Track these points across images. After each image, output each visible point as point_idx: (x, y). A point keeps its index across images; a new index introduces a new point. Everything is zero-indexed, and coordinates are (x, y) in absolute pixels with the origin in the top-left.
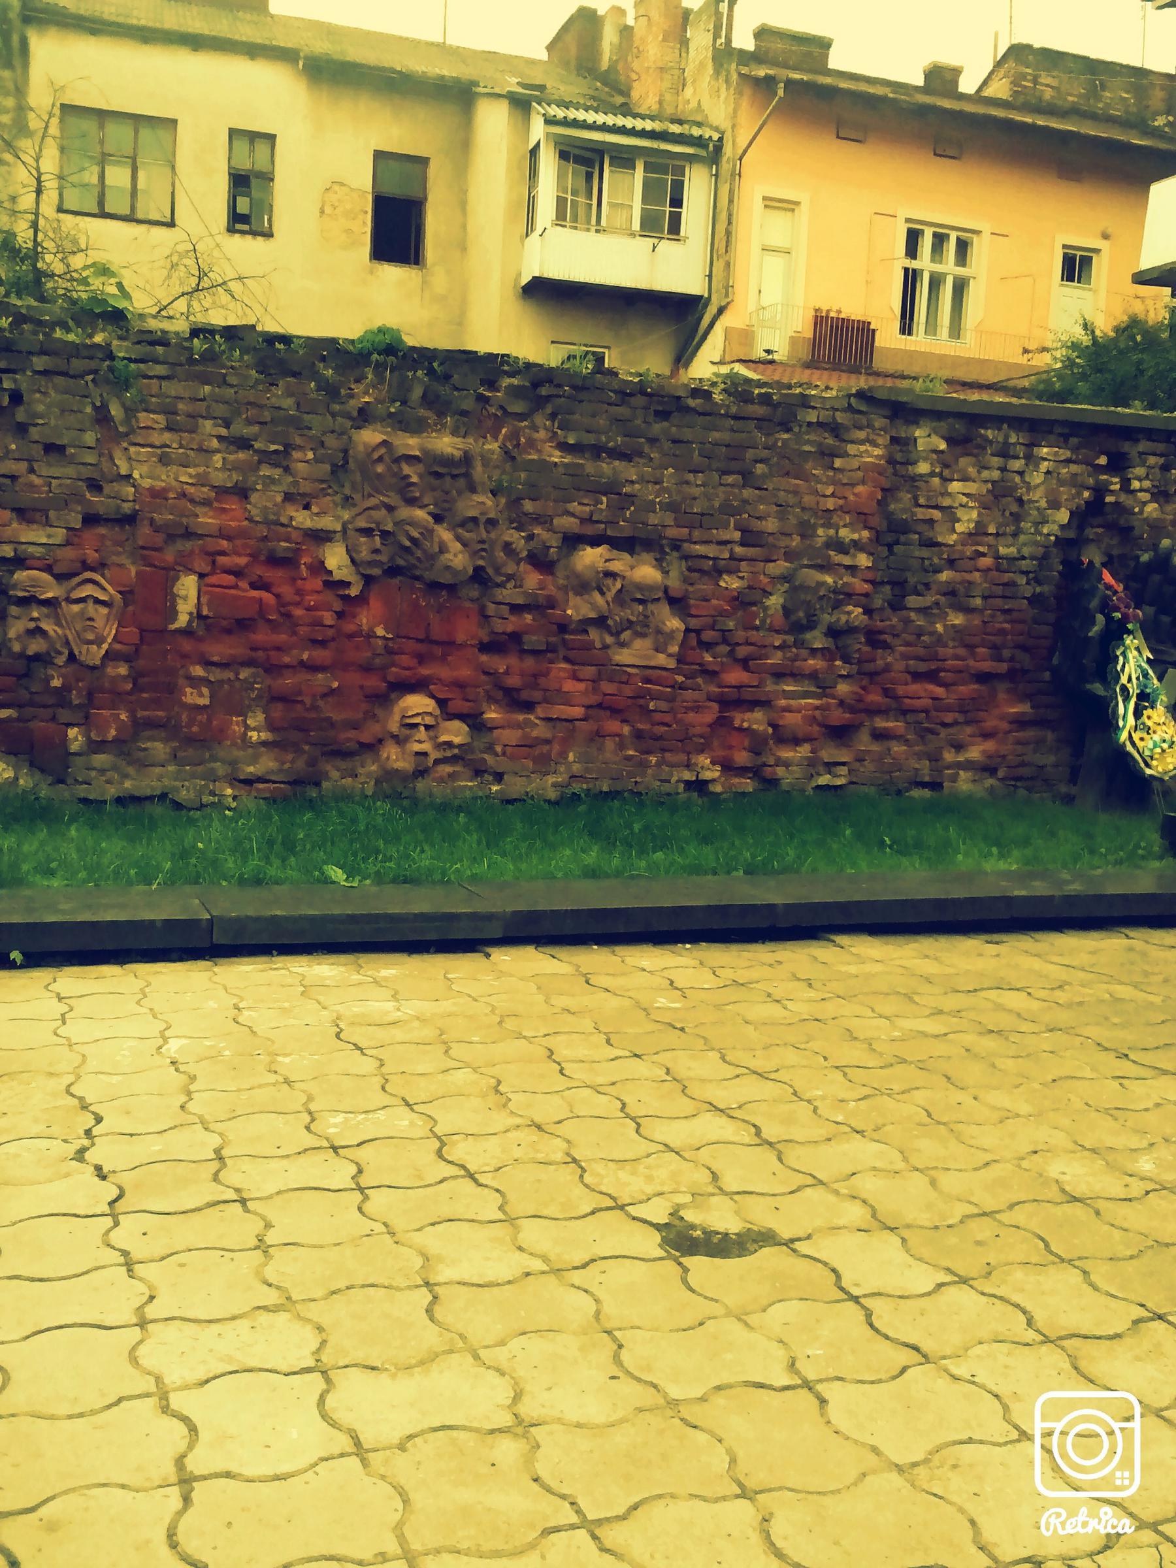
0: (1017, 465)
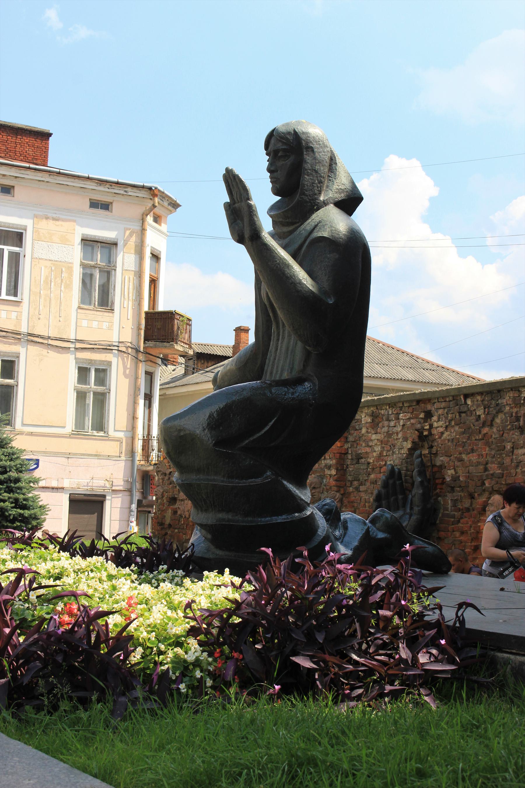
0: (392, 424)
